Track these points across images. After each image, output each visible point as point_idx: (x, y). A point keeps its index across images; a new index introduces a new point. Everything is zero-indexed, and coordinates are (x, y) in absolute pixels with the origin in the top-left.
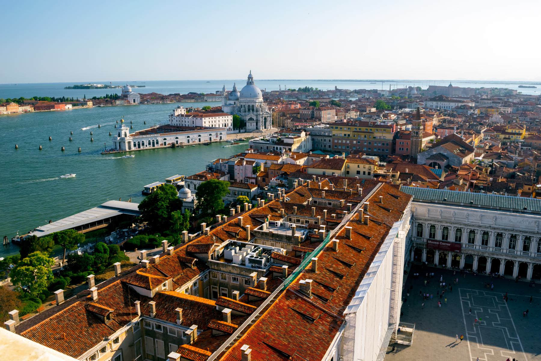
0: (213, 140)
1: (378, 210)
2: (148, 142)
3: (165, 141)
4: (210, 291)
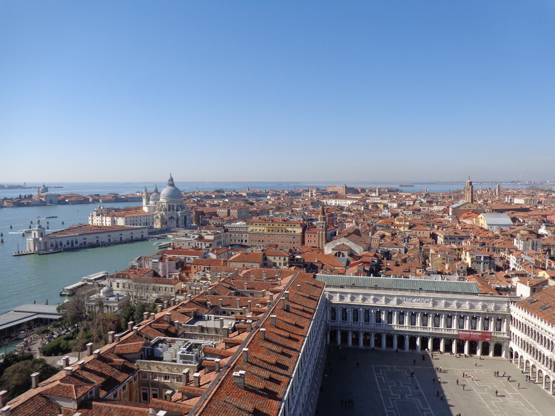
2: (66, 242)
3: (85, 240)
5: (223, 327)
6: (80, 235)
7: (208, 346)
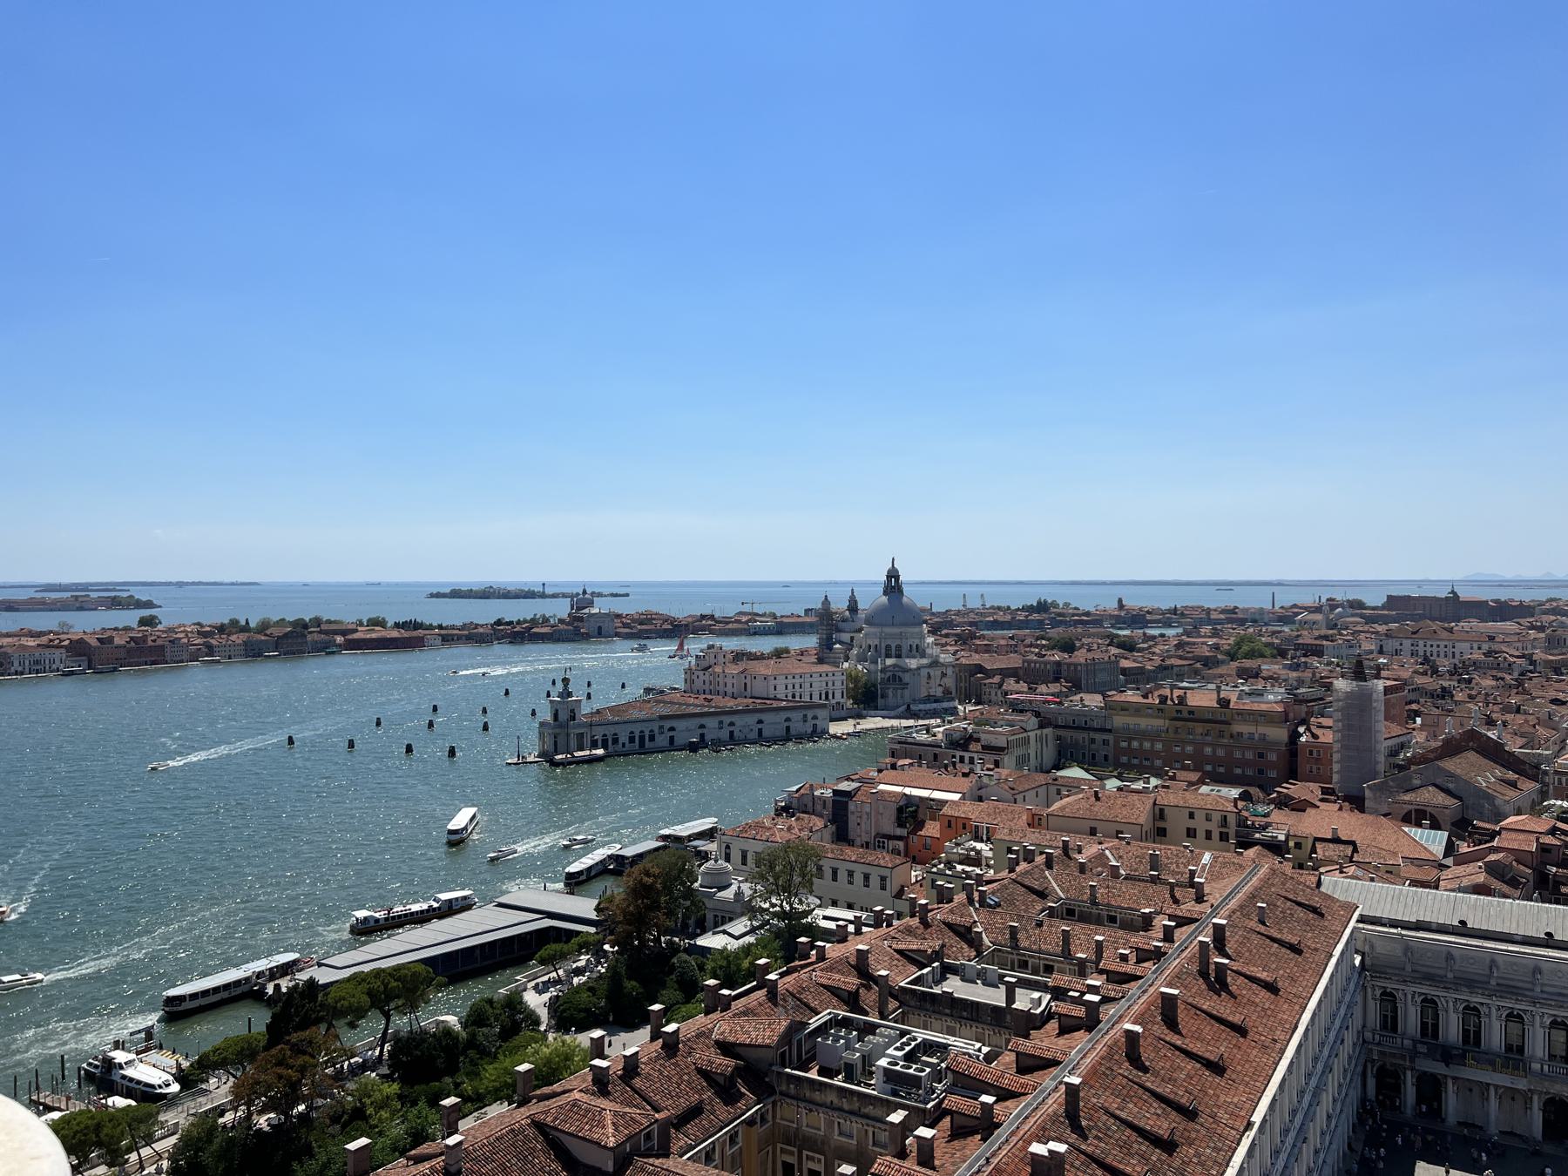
0: (793, 732)
4: (774, 1162)
5: (1014, 1006)
6: (662, 718)
7: (965, 1054)
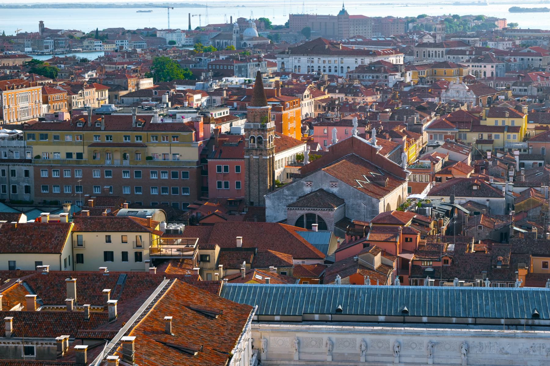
1: (163, 355)
